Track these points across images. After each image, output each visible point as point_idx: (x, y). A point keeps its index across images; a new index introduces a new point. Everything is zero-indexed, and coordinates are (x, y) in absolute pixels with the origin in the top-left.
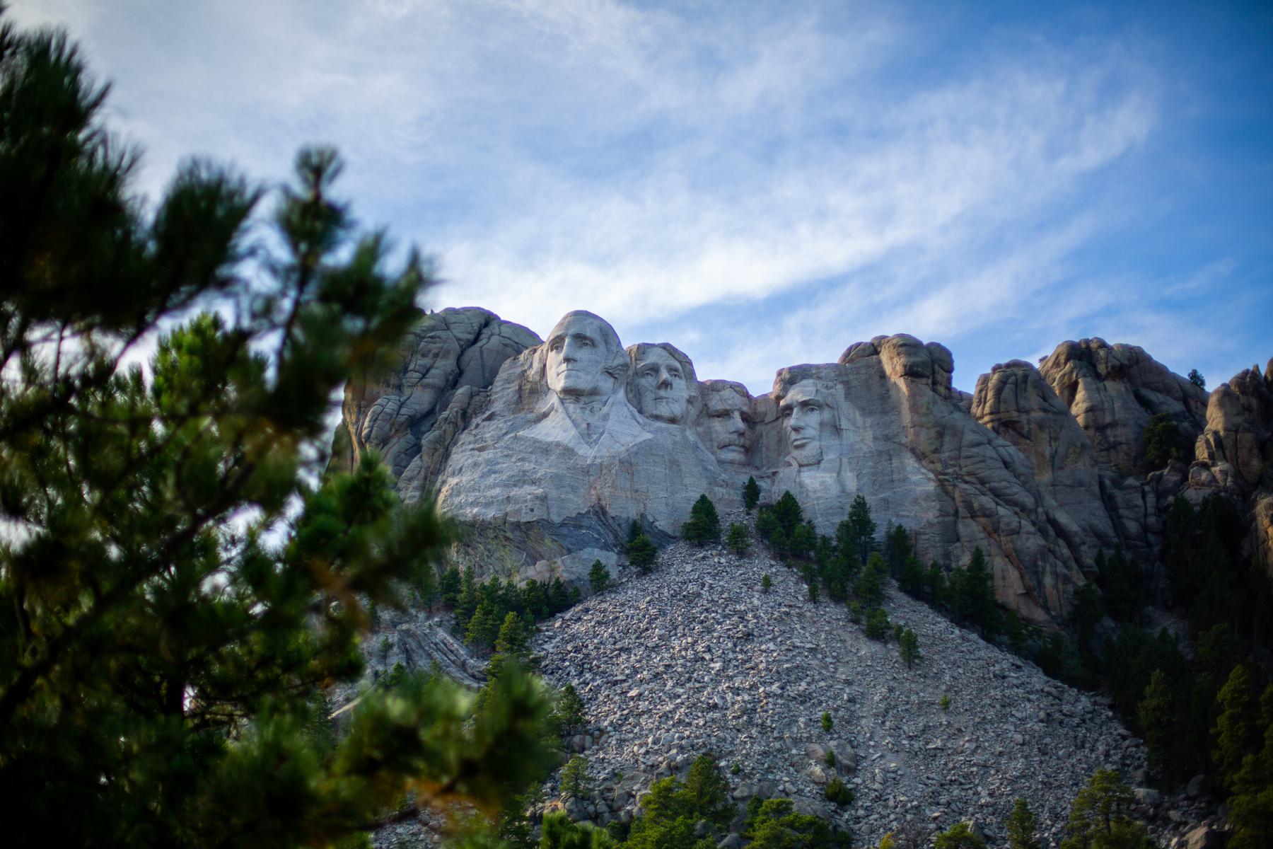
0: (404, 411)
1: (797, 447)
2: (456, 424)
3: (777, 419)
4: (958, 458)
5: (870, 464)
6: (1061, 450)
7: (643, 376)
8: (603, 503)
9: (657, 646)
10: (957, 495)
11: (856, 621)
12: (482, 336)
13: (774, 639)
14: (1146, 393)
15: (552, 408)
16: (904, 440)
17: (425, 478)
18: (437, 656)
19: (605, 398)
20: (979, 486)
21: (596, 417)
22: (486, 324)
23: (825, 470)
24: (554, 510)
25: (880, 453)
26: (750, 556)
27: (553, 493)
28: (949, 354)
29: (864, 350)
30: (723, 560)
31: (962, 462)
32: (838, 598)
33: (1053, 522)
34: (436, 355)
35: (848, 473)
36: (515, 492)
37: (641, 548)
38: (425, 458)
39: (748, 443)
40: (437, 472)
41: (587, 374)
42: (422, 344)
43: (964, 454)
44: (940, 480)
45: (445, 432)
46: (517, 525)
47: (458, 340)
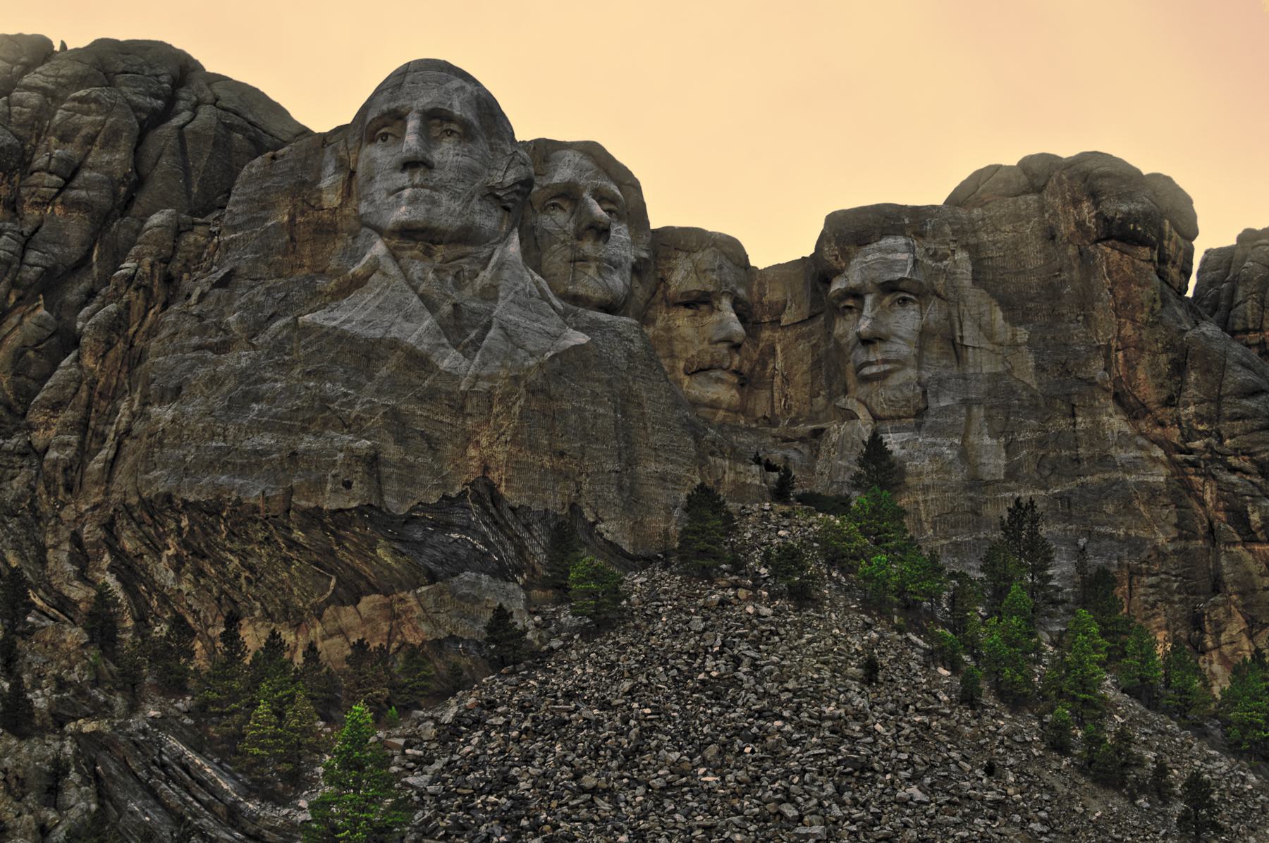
0: (33, 256)
1: (867, 379)
2: (149, 297)
3: (812, 317)
7: (544, 209)
8: (494, 476)
9: (669, 785)
10: (1208, 497)
12: (181, 104)
13: (915, 779)
15: (375, 267)
17: (89, 406)
19: (487, 251)
20: (1258, 480)
21: (468, 292)
24: (392, 487)
26: (817, 604)
27: (392, 451)
28: (1190, 201)
30: (765, 611)
31: (1225, 426)
35: (987, 440)
36: (306, 443)
38: (88, 361)
39: (746, 367)
40: (113, 395)
41: (455, 196)
43: (1227, 411)
44: (1174, 463)
45: (128, 306)
47: (136, 109)
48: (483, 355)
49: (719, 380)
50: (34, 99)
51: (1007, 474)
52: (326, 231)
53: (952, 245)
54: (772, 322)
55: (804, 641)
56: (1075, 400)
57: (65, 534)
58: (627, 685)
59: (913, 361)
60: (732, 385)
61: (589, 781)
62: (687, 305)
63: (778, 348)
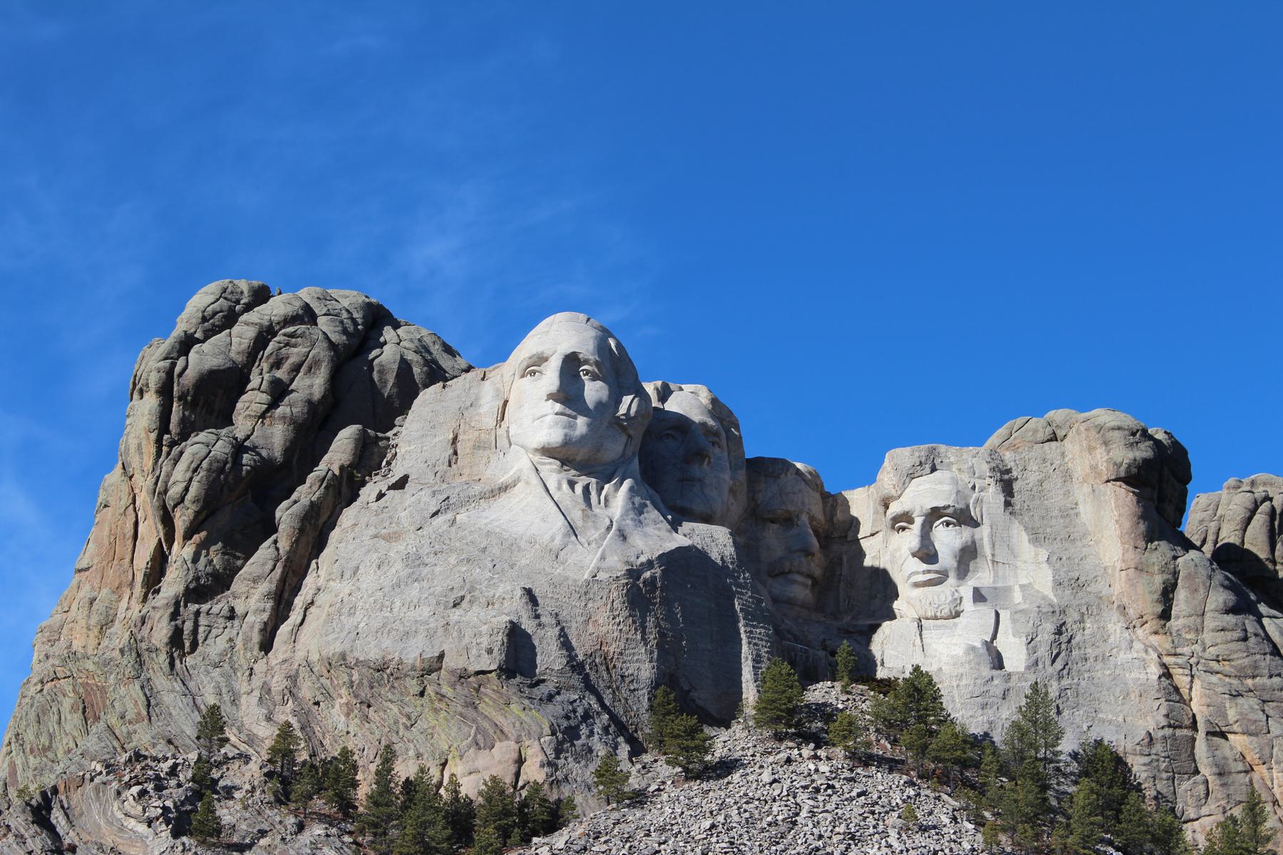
4: (1199, 630)
5: (1049, 627)
28: (1185, 453)
29: (1035, 431)
30: (824, 768)
35: (1012, 639)
39: (818, 572)
42: (271, 346)
46: (463, 676)
48: (604, 551)
49: (794, 582)
50: (251, 333)
51: (1028, 668)
53: (988, 480)
54: (840, 537)
55: (854, 794)
56: (1084, 610)
58: (707, 824)
59: (952, 575)
60: (805, 586)
62: (773, 522)
63: (845, 559)
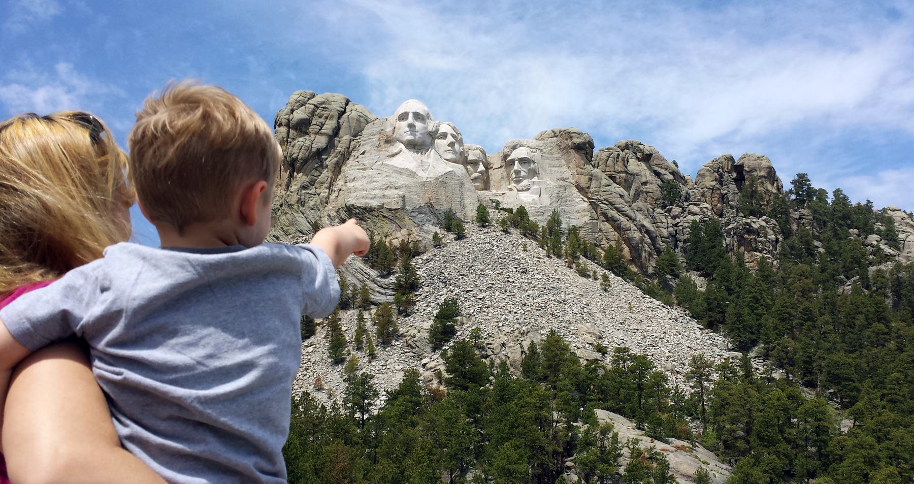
3: (501, 167)
6: (632, 192)
11: (571, 268)
14: (656, 168)
16: (572, 181)
18: (360, 276)
22: (347, 104)
23: (532, 193)
24: (407, 204)
25: (560, 187)
27: (407, 195)
32: (559, 257)
33: (643, 226)
34: (327, 118)
36: (387, 193)
37: (452, 224)
46: (390, 210)
52: (389, 141)
57: (326, 213)
61: (462, 272)
